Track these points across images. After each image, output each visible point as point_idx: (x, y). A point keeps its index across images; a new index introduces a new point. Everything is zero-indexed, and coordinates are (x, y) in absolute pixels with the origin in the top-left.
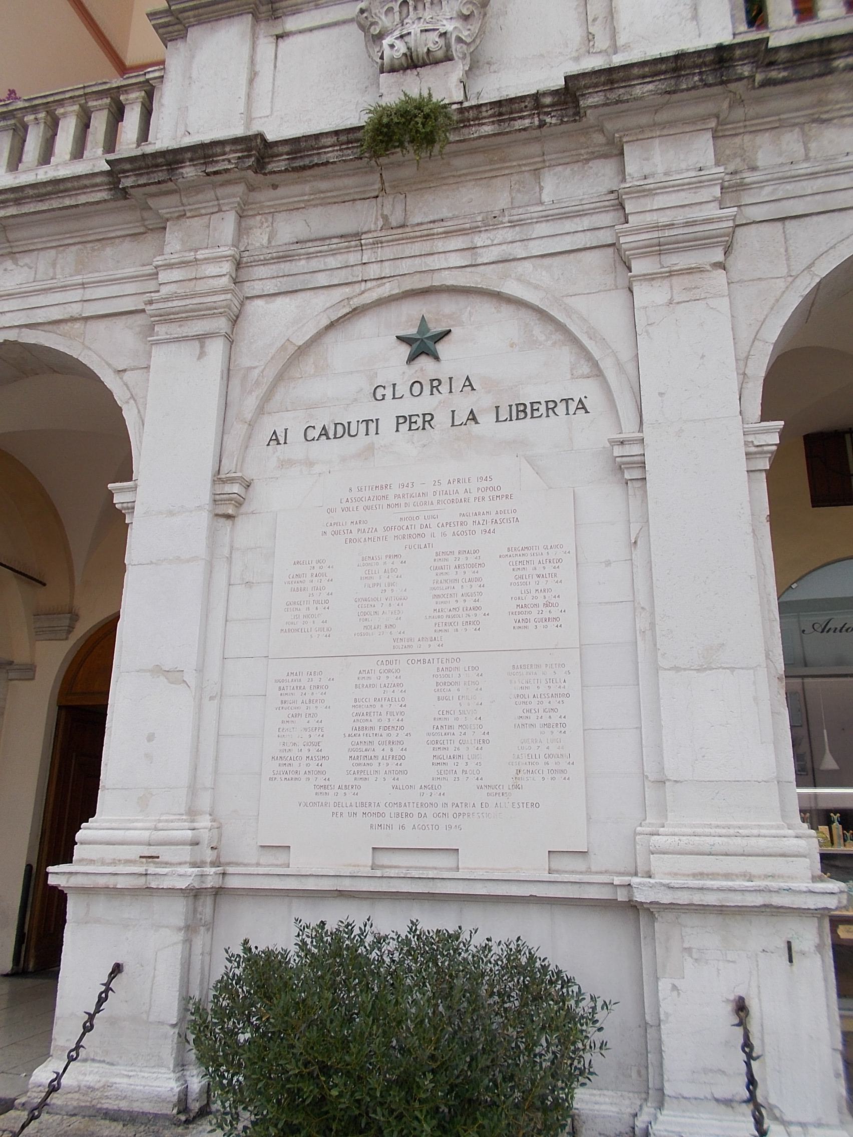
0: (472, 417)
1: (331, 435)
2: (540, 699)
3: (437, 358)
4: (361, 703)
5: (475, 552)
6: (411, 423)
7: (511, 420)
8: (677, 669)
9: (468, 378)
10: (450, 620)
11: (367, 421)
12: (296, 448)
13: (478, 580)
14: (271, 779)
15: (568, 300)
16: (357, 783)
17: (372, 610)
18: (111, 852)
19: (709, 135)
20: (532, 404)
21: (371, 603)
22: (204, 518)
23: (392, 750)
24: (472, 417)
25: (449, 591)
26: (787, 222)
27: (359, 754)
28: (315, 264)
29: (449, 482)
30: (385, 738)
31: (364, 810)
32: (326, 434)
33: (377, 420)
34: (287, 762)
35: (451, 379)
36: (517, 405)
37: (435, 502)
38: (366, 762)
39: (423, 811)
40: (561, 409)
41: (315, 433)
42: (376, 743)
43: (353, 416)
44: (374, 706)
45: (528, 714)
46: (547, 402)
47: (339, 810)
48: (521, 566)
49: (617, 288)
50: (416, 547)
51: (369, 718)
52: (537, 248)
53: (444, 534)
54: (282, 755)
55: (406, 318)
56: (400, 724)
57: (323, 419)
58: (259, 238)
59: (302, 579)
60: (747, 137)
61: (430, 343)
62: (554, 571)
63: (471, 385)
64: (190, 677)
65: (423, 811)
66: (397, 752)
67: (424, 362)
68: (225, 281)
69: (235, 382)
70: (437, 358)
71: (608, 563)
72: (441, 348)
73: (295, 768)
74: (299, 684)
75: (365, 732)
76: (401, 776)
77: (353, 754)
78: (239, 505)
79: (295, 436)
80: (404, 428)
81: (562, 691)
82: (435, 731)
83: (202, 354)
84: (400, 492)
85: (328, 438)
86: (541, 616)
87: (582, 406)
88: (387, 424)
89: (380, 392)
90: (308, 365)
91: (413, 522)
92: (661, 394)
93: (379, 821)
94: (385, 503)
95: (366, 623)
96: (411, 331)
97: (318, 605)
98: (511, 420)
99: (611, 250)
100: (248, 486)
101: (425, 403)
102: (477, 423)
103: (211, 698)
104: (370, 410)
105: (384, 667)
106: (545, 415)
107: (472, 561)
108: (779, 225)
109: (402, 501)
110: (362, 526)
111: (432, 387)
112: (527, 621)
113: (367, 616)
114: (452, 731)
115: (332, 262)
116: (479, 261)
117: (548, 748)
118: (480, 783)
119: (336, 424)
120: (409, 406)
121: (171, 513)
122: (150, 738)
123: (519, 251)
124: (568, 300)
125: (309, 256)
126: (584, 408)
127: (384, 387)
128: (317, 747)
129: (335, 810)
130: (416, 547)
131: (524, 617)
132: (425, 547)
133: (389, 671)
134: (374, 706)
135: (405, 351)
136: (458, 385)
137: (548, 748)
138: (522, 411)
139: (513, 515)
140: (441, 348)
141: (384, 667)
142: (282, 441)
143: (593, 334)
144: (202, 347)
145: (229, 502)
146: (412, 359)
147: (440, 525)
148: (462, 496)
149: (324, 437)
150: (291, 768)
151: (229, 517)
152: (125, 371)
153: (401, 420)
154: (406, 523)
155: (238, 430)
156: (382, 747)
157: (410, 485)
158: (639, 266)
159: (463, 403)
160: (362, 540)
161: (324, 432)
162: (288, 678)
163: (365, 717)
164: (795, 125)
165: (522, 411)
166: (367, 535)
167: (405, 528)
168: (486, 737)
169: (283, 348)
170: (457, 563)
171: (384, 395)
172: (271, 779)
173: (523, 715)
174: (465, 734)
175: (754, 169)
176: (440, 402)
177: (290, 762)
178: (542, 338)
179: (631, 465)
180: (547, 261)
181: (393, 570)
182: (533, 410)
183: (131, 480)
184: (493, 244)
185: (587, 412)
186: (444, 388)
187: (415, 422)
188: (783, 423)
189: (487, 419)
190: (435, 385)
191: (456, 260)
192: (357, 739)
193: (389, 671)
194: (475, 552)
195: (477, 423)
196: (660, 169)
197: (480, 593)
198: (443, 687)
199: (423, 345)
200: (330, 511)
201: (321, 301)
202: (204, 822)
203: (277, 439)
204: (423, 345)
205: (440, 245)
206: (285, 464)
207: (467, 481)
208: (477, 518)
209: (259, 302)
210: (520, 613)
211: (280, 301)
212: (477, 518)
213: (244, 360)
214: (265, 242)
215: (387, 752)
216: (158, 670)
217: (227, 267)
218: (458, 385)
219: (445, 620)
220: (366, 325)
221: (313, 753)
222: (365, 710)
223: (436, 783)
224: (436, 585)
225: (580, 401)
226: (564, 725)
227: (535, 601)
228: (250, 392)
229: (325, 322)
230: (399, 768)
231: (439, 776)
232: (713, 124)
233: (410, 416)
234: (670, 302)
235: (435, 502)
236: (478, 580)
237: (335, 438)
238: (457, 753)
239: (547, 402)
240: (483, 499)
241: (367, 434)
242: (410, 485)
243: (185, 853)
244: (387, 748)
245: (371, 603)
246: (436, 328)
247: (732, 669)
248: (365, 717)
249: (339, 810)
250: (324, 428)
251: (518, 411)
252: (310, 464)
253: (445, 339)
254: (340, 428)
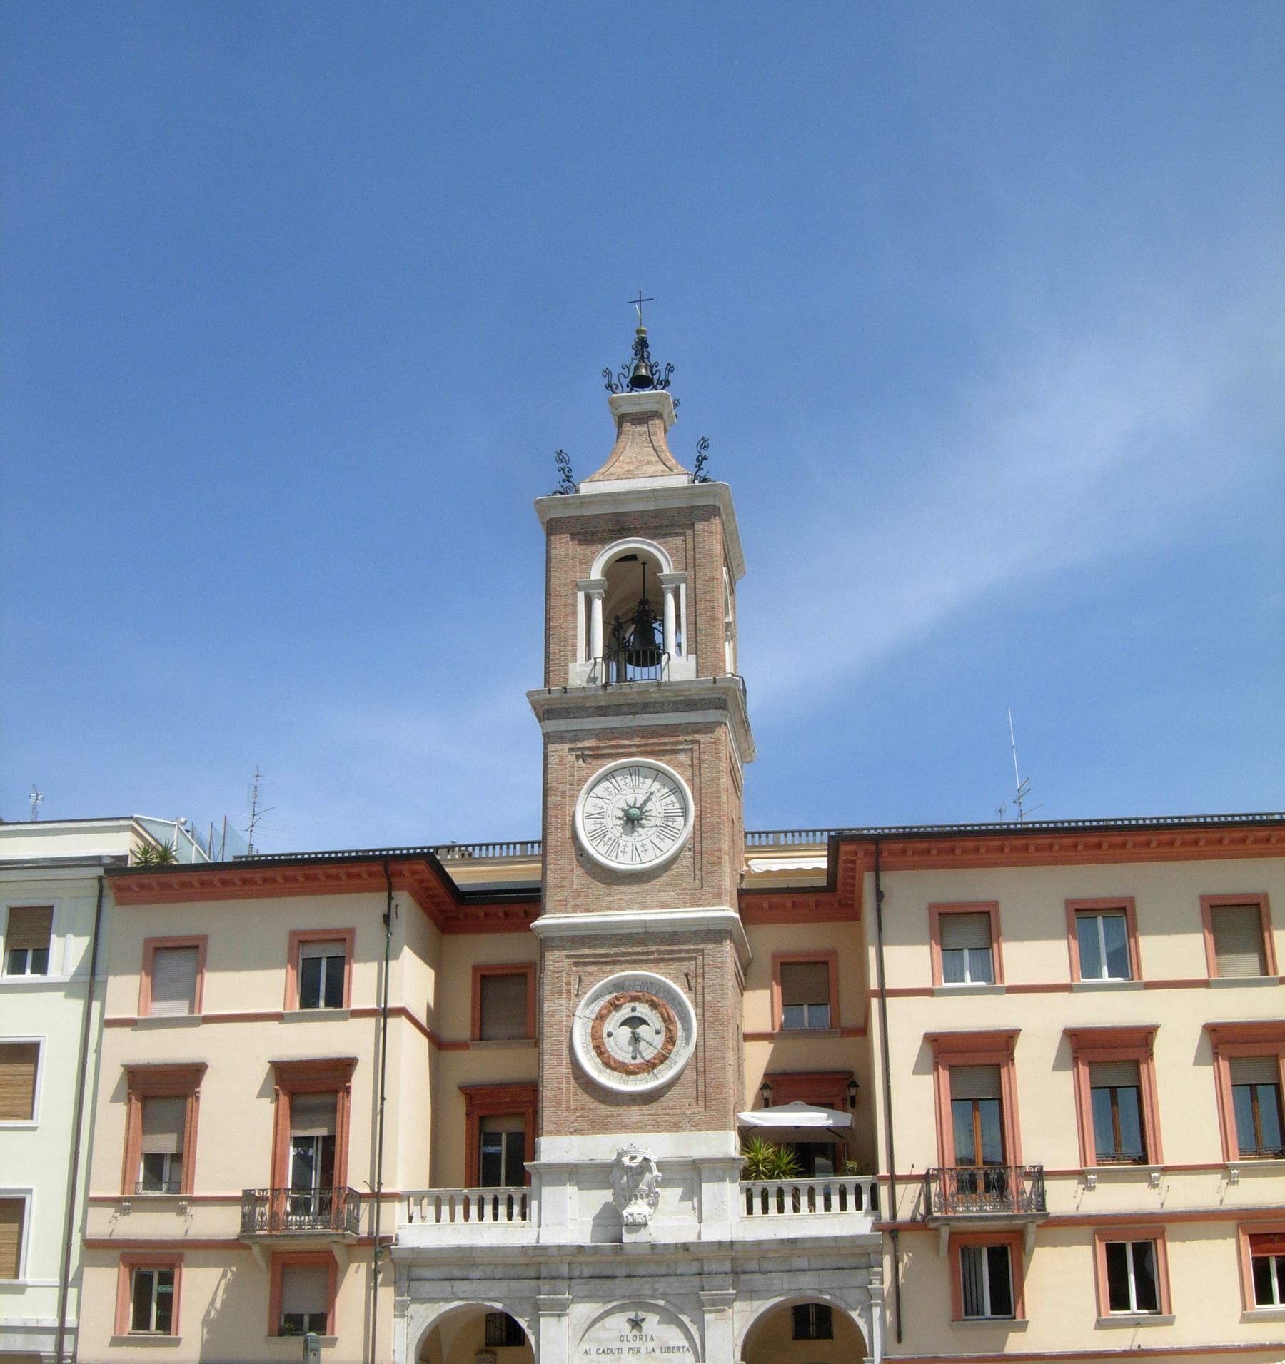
12: (593, 1355)
43: (614, 1346)
72: (643, 1325)
79: (593, 1352)
88: (625, 1350)
101: (637, 1344)
104: (618, 1344)
120: (632, 1344)
123: (668, 1291)
138: (669, 1349)
153: (630, 1349)
159: (651, 1345)
165: (669, 1349)
189: (658, 1351)
199: (636, 1324)
204: (636, 1324)
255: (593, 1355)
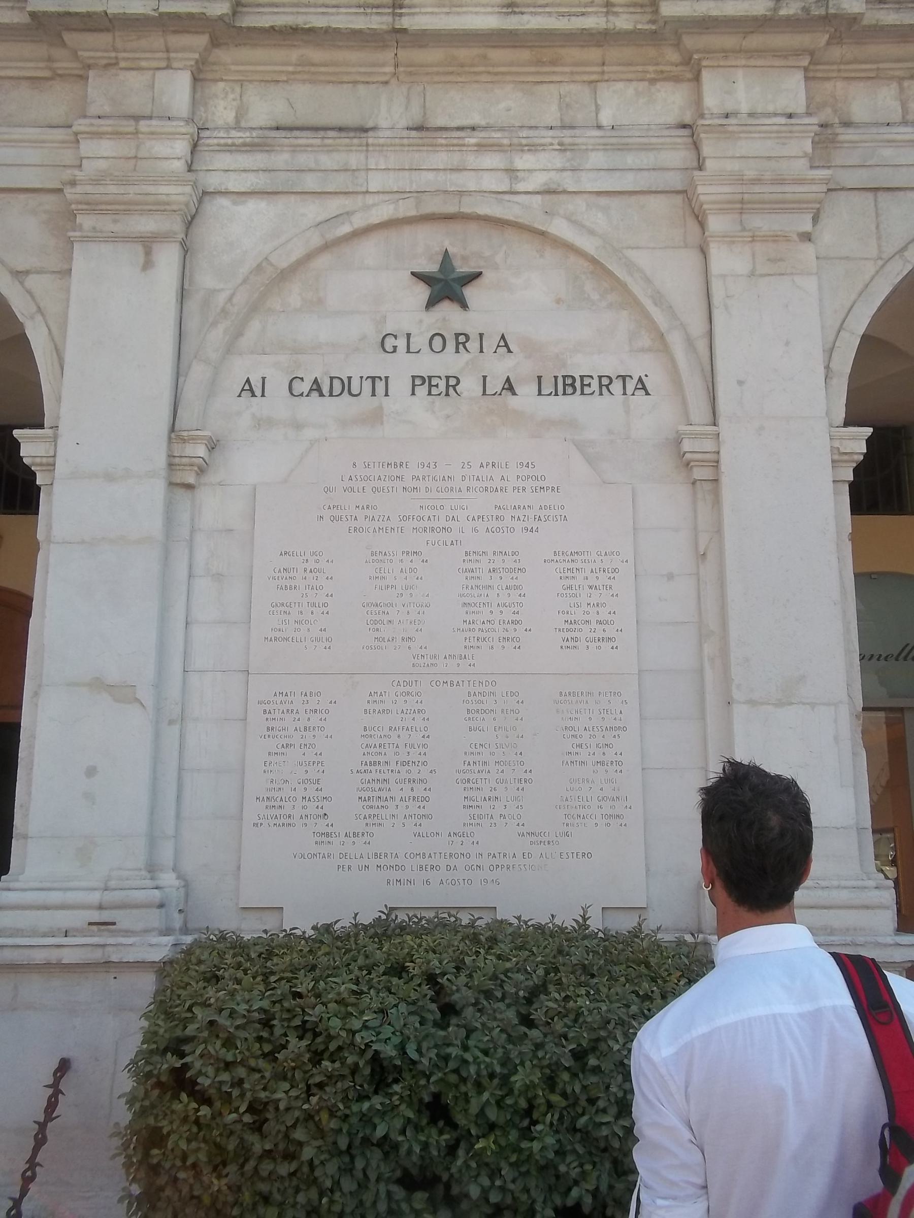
0: (509, 386)
1: (326, 390)
2: (592, 733)
3: (464, 306)
4: (372, 733)
5: (514, 554)
6: (430, 386)
7: (556, 394)
8: (752, 703)
9: (503, 337)
10: (484, 635)
11: (373, 379)
12: (277, 402)
13: (517, 587)
14: (255, 825)
15: (631, 254)
16: (369, 829)
17: (386, 618)
18: (45, 919)
19: (799, 76)
20: (582, 377)
21: (383, 609)
22: (158, 487)
23: (412, 789)
24: (509, 386)
25: (483, 599)
26: (880, 194)
27: (370, 794)
28: (304, 160)
29: (482, 466)
30: (404, 775)
31: (378, 862)
32: (319, 391)
33: (387, 378)
34: (275, 804)
35: (481, 335)
36: (564, 377)
37: (464, 489)
38: (380, 804)
39: (453, 862)
40: (617, 387)
41: (305, 387)
42: (392, 781)
44: (389, 737)
45: (578, 750)
46: (600, 377)
47: (347, 862)
48: (569, 574)
49: (686, 247)
50: (441, 543)
51: (382, 750)
52: (590, 183)
53: (475, 530)
54: (270, 794)
55: (425, 248)
56: (422, 758)
57: (314, 369)
58: (222, 111)
59: (292, 575)
60: (840, 84)
61: (456, 286)
62: (609, 582)
63: (506, 345)
64: (146, 694)
65: (453, 862)
66: (419, 791)
67: (447, 309)
68: (179, 166)
69: (192, 305)
70: (464, 306)
71: (670, 577)
73: (287, 810)
74: (290, 707)
75: (378, 768)
76: (424, 821)
77: (364, 794)
78: (201, 471)
80: (422, 391)
81: (618, 724)
82: (466, 767)
83: (148, 264)
84: (420, 473)
85: (321, 395)
86: (593, 635)
87: (642, 385)
89: (389, 343)
90: (294, 294)
91: (435, 512)
92: (740, 383)
93: (398, 875)
94: (399, 484)
95: (378, 635)
96: (431, 267)
97: (314, 609)
98: (556, 394)
99: (678, 199)
100: (213, 446)
101: (447, 363)
102: (514, 394)
103: (171, 722)
105: (401, 689)
106: (597, 392)
107: (510, 564)
108: (870, 195)
109: (420, 484)
110: (370, 513)
111: (458, 344)
112: (576, 639)
113: (378, 626)
114: (487, 768)
115: (327, 161)
116: (521, 187)
117: (601, 789)
118: (521, 829)
119: (332, 378)
121: (110, 477)
122: (91, 772)
123: (568, 182)
124: (631, 254)
125: (295, 149)
126: (644, 388)
127: (396, 337)
128: (316, 786)
129: (341, 862)
130: (441, 543)
131: (574, 635)
132: (452, 544)
133: (408, 693)
134: (389, 737)
135: (422, 292)
136: (490, 343)
137: (601, 789)
138: (570, 385)
139: (561, 512)
140: (470, 292)
141: (401, 689)
142: (258, 392)
143: (659, 299)
144: (148, 253)
145: (187, 468)
146: (431, 303)
147: (470, 518)
148: (497, 483)
149: (315, 394)
150: (282, 812)
151: (189, 487)
152: (27, 273)
153: (418, 381)
154: (426, 513)
155: (198, 373)
156: (400, 786)
157: (432, 465)
158: (715, 224)
159: (500, 367)
160: (371, 530)
161: (316, 387)
162: (275, 699)
163: (378, 750)
164: (892, 78)
165: (570, 385)
166: (376, 525)
167: (426, 518)
168: (528, 776)
169: (259, 269)
170: (492, 566)
171: (395, 347)
172: (255, 825)
173: (572, 750)
174: (502, 771)
175: (847, 124)
176: (467, 363)
177: (282, 804)
178: (595, 296)
179: (702, 463)
180: (603, 201)
181: (411, 570)
182: (583, 385)
183: (41, 426)
184: (539, 170)
185: (647, 394)
186: (473, 345)
187: (437, 386)
188: (871, 430)
189: (527, 390)
190: (461, 340)
191: (491, 182)
192: (368, 777)
193: (408, 693)
194: (514, 554)
195: (514, 394)
196: (744, 108)
197: (520, 604)
198: (476, 715)
199: (446, 286)
200: (328, 490)
201: (313, 211)
202: (168, 879)
203: (251, 390)
204: (446, 286)
205: (472, 160)
206: (262, 423)
207: (504, 465)
208: (516, 513)
209: (224, 201)
210: (568, 630)
211: (252, 205)
212: (516, 513)
213: (205, 280)
214: (229, 117)
215: (407, 793)
216: (98, 685)
217: (181, 147)
218: (490, 343)
219: (477, 634)
220: (369, 250)
221: (311, 792)
222: (377, 741)
223: (468, 829)
224: (466, 592)
225: (640, 379)
226: (619, 763)
227: (587, 617)
228: (214, 324)
229: (316, 240)
230: (422, 812)
231: (472, 821)
232: (805, 63)
233: (430, 378)
234: (752, 274)
235: (464, 489)
236: (517, 587)
237: (331, 395)
238: (493, 794)
239: (600, 377)
240: (524, 489)
241: (374, 395)
242: (432, 465)
243: (154, 918)
244: (407, 786)
245: (383, 609)
246: (462, 268)
247: (813, 705)
248: (378, 750)
249: (347, 862)
250: (316, 381)
251: (565, 385)
252: (298, 426)
253: (475, 283)
254: (337, 384)
255: (277, 402)
